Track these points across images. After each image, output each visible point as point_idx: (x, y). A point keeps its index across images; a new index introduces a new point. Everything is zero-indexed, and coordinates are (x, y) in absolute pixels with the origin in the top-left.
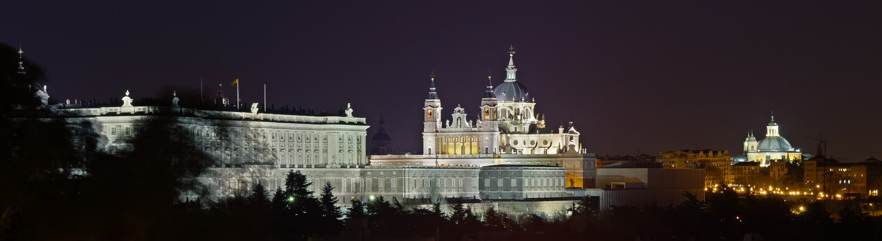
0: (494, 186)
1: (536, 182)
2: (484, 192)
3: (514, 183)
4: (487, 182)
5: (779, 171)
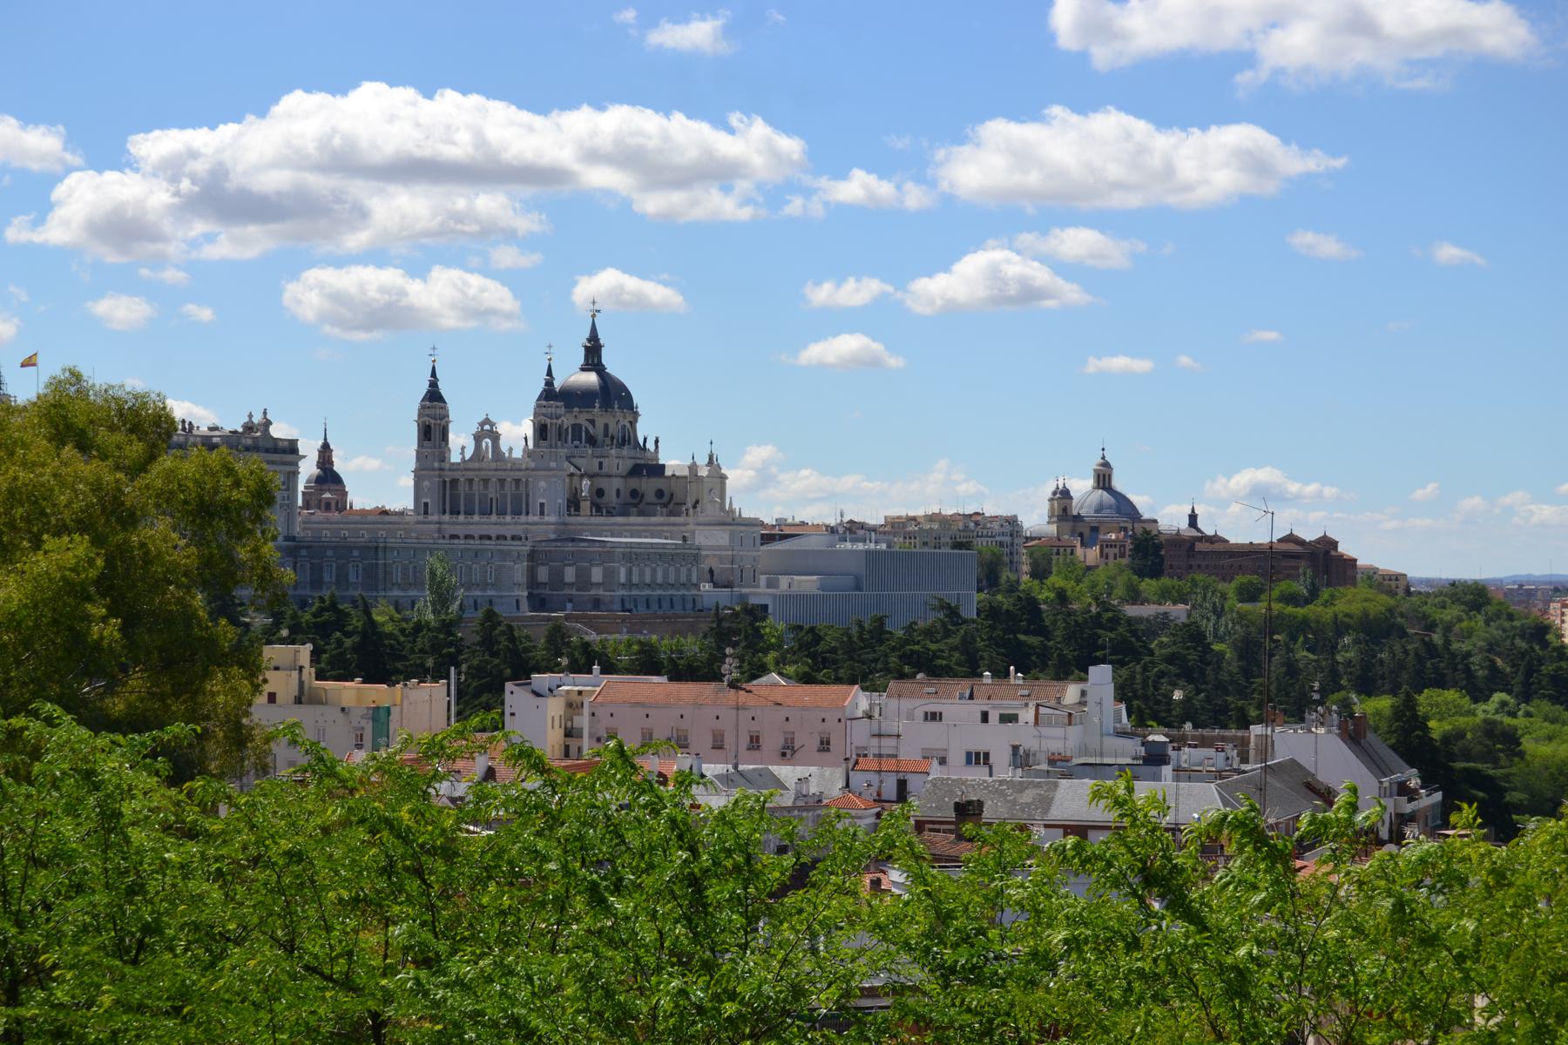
0: (557, 580)
1: (642, 574)
2: (535, 592)
5: (1115, 558)
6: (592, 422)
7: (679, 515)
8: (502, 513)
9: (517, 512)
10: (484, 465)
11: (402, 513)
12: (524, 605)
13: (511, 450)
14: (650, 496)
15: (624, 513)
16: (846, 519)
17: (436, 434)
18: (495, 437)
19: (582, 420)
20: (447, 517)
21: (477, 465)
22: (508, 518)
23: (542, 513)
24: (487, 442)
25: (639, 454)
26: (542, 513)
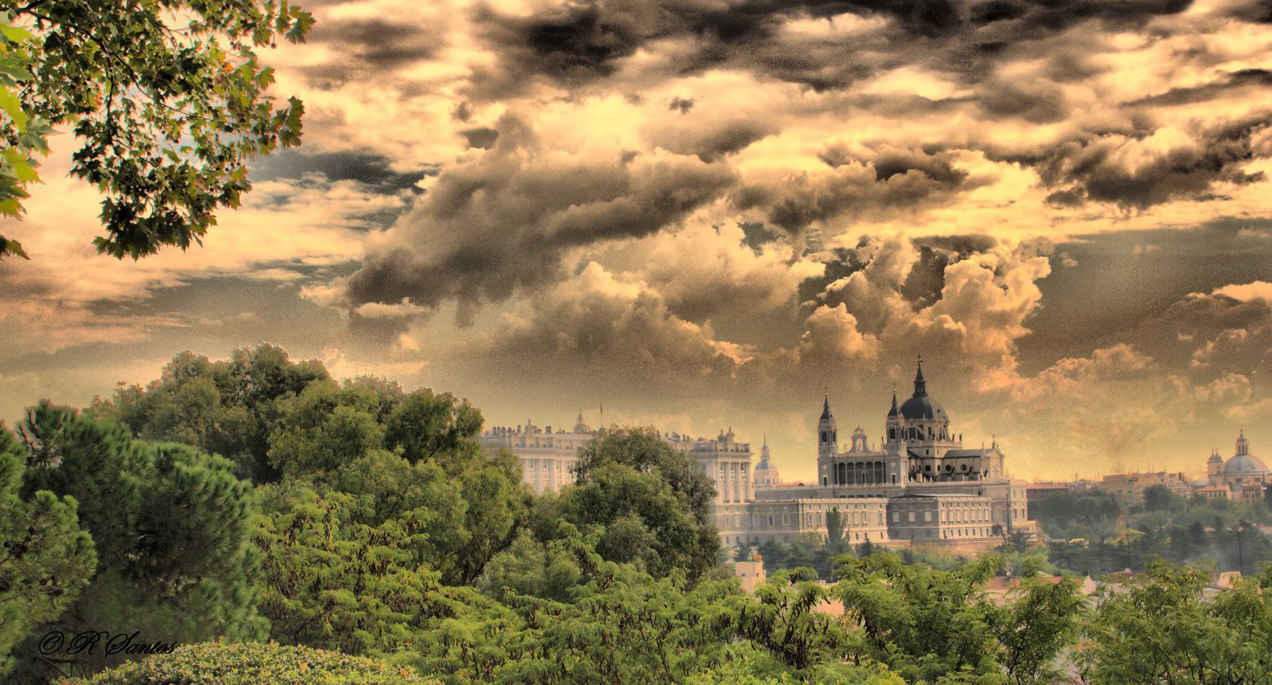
3: (928, 516)
4: (896, 518)
6: (921, 427)
7: (976, 479)
8: (870, 482)
9: (879, 482)
10: (858, 454)
11: (811, 486)
12: (885, 534)
13: (874, 445)
14: (958, 469)
15: (942, 480)
16: (1079, 478)
17: (830, 437)
18: (864, 439)
19: (915, 426)
20: (838, 486)
21: (852, 455)
22: (874, 485)
23: (894, 481)
24: (859, 441)
25: (949, 444)
26: (894, 481)
